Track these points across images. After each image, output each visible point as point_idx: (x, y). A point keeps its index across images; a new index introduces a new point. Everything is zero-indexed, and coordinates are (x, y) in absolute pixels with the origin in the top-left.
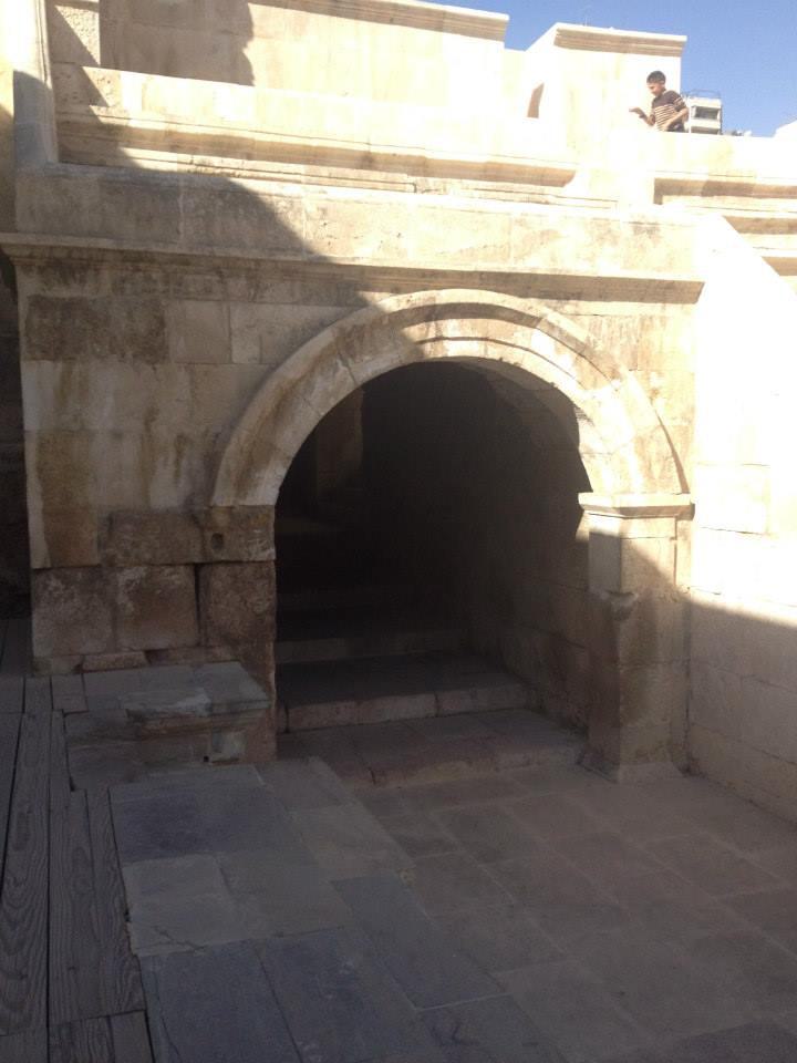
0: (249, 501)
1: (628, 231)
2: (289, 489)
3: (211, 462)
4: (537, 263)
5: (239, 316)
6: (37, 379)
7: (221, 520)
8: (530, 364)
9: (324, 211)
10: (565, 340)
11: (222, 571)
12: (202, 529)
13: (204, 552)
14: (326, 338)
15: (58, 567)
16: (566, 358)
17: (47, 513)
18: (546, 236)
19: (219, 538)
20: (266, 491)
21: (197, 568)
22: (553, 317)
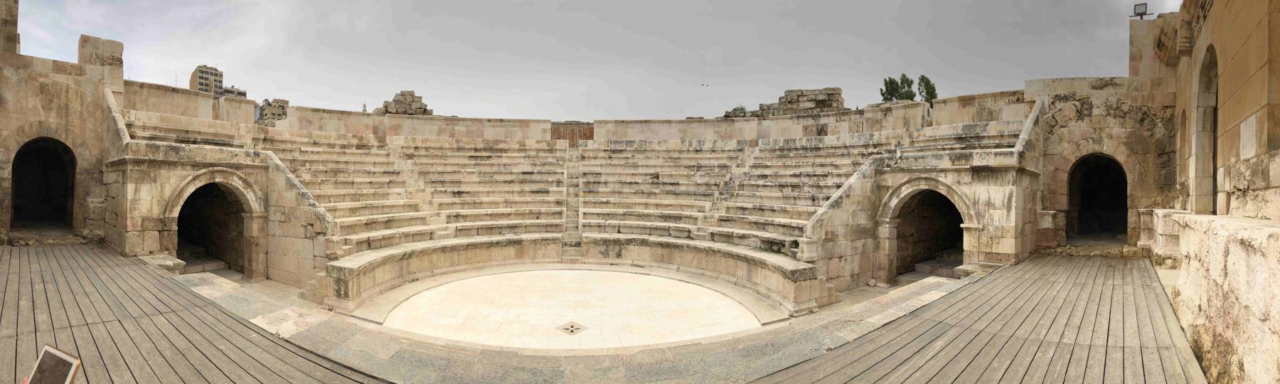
1: (252, 155)
4: (234, 161)
5: (172, 173)
6: (130, 187)
10: (240, 178)
11: (166, 232)
13: (162, 228)
14: (190, 178)
16: (240, 182)
18: (236, 155)
20: (176, 213)
22: (238, 173)
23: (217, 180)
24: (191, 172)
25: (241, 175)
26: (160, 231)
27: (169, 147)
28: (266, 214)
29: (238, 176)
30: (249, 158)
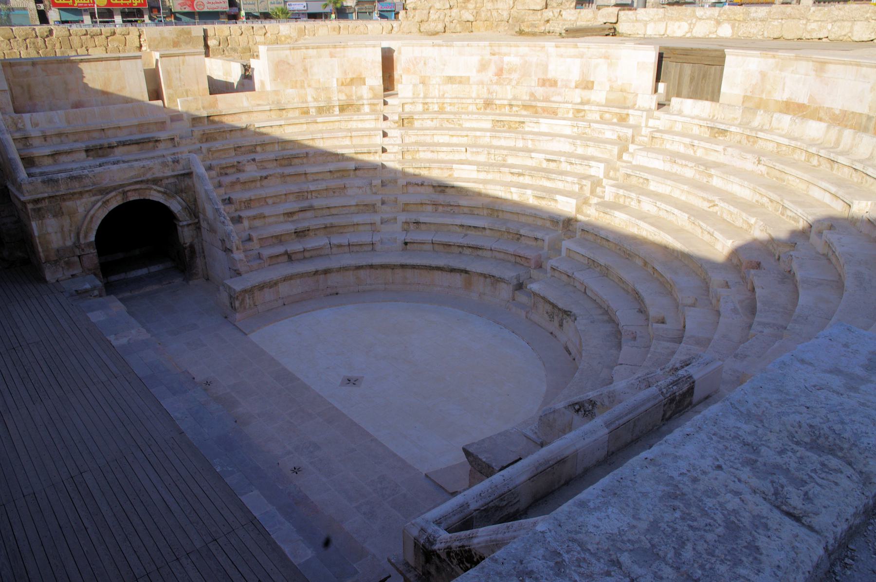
0: (88, 241)
2: (96, 236)
3: (78, 234)
4: (149, 176)
5: (78, 202)
7: (83, 246)
8: (151, 198)
9: (94, 176)
10: (159, 192)
12: (79, 248)
14: (100, 204)
15: (47, 261)
16: (160, 195)
17: (43, 251)
18: (150, 169)
19: (83, 250)
20: (92, 238)
21: (79, 256)
23: (131, 199)
24: (99, 197)
25: (159, 189)
26: (79, 256)
27: (69, 178)
28: (196, 221)
29: (155, 190)
30: (167, 168)
